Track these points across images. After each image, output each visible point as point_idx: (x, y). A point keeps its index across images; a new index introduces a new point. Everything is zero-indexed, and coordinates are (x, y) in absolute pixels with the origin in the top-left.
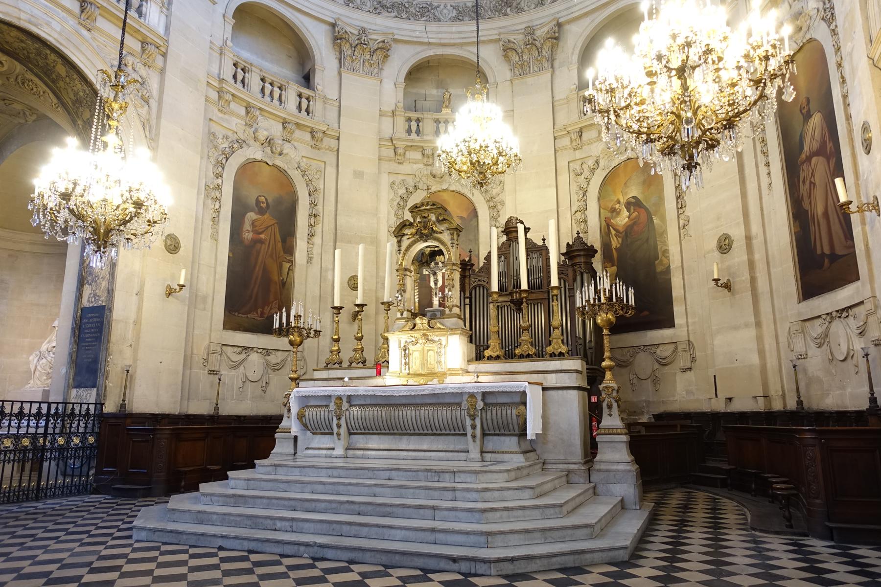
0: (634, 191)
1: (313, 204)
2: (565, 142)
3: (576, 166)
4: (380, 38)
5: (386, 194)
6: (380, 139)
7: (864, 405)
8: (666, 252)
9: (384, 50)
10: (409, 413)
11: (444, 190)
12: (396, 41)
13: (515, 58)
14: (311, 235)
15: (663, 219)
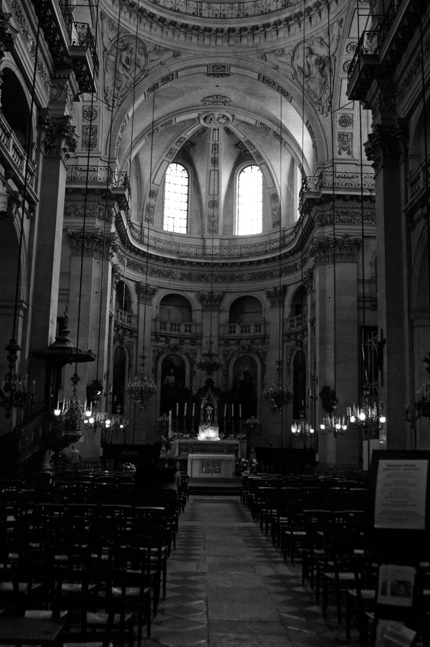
0: (246, 369)
1: (130, 361)
2: (222, 342)
3: (226, 352)
4: (154, 287)
5: (152, 355)
6: (152, 332)
7: (303, 448)
8: (256, 393)
9: (154, 292)
10: (211, 447)
11: (172, 355)
12: (160, 287)
13: (205, 303)
14: (129, 374)
15: (256, 381)
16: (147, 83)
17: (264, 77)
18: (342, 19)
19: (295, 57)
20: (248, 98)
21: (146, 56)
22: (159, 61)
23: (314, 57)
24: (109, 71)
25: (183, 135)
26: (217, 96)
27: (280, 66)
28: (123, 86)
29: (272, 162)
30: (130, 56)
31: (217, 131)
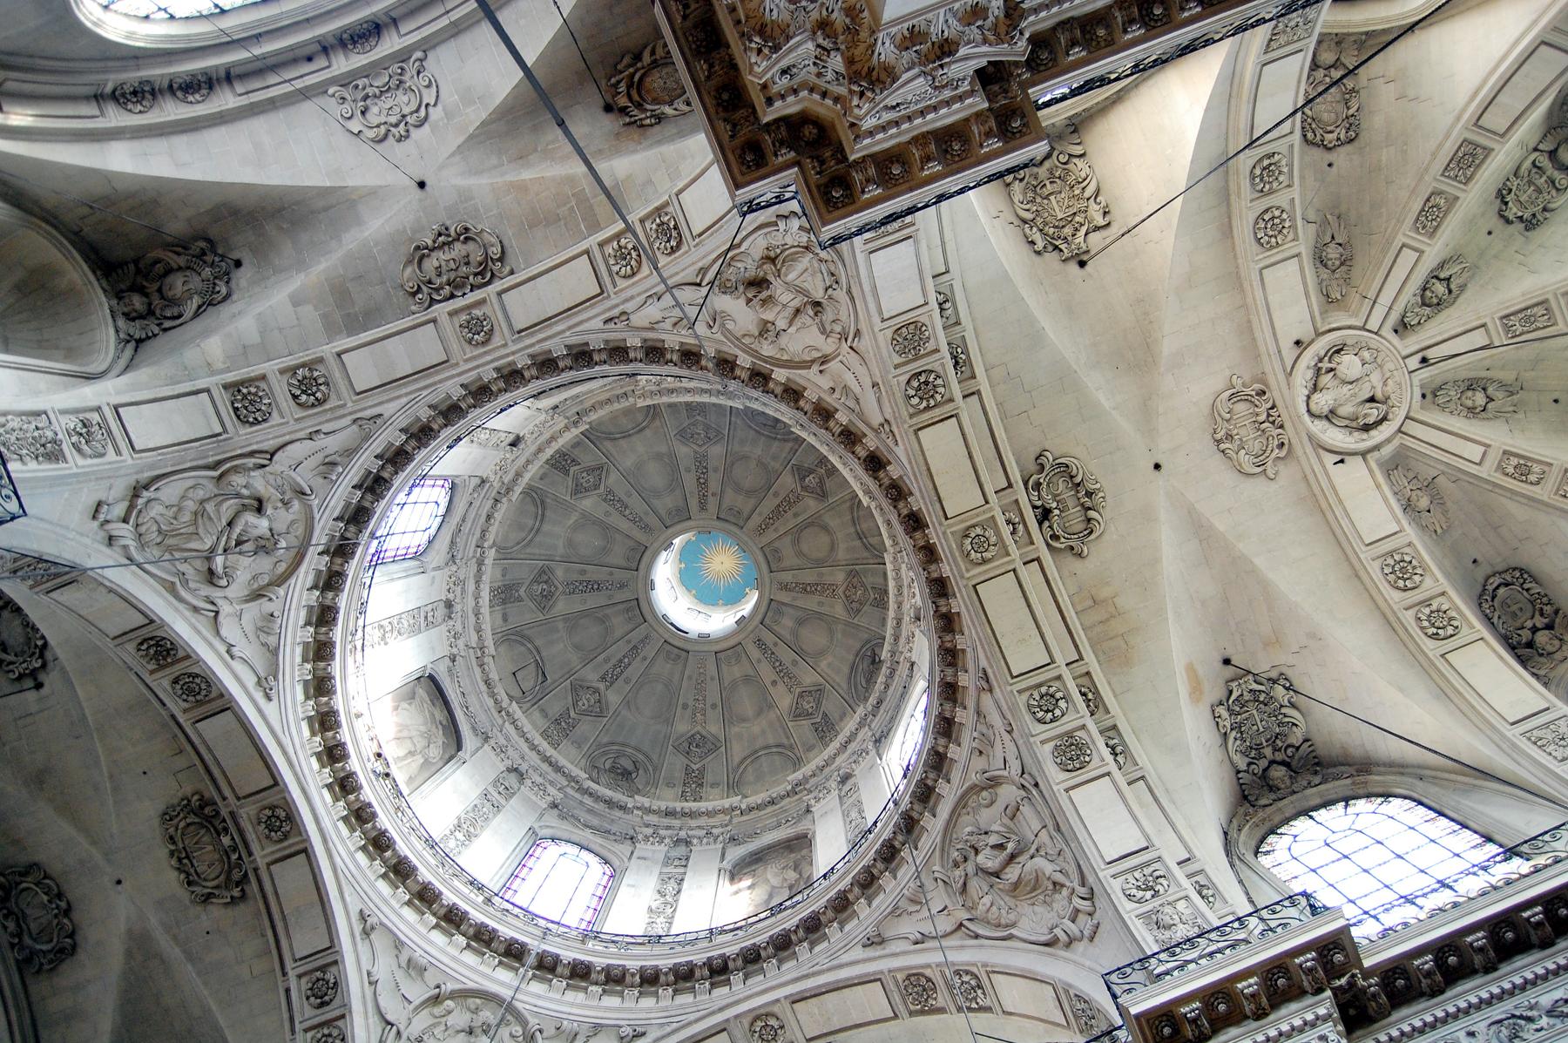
16: (1055, 777)
17: (911, 416)
18: (606, 322)
19: (816, 355)
20: (1168, 347)
21: (994, 782)
22: (1006, 737)
23: (769, 315)
24: (1012, 917)
25: (1483, 471)
26: (1219, 442)
27: (867, 382)
28: (1048, 868)
29: (1462, 98)
30: (993, 840)
31: (1430, 354)
